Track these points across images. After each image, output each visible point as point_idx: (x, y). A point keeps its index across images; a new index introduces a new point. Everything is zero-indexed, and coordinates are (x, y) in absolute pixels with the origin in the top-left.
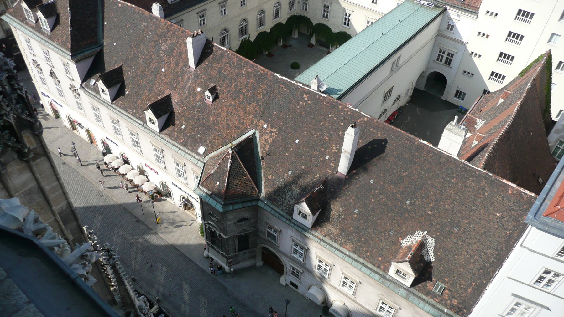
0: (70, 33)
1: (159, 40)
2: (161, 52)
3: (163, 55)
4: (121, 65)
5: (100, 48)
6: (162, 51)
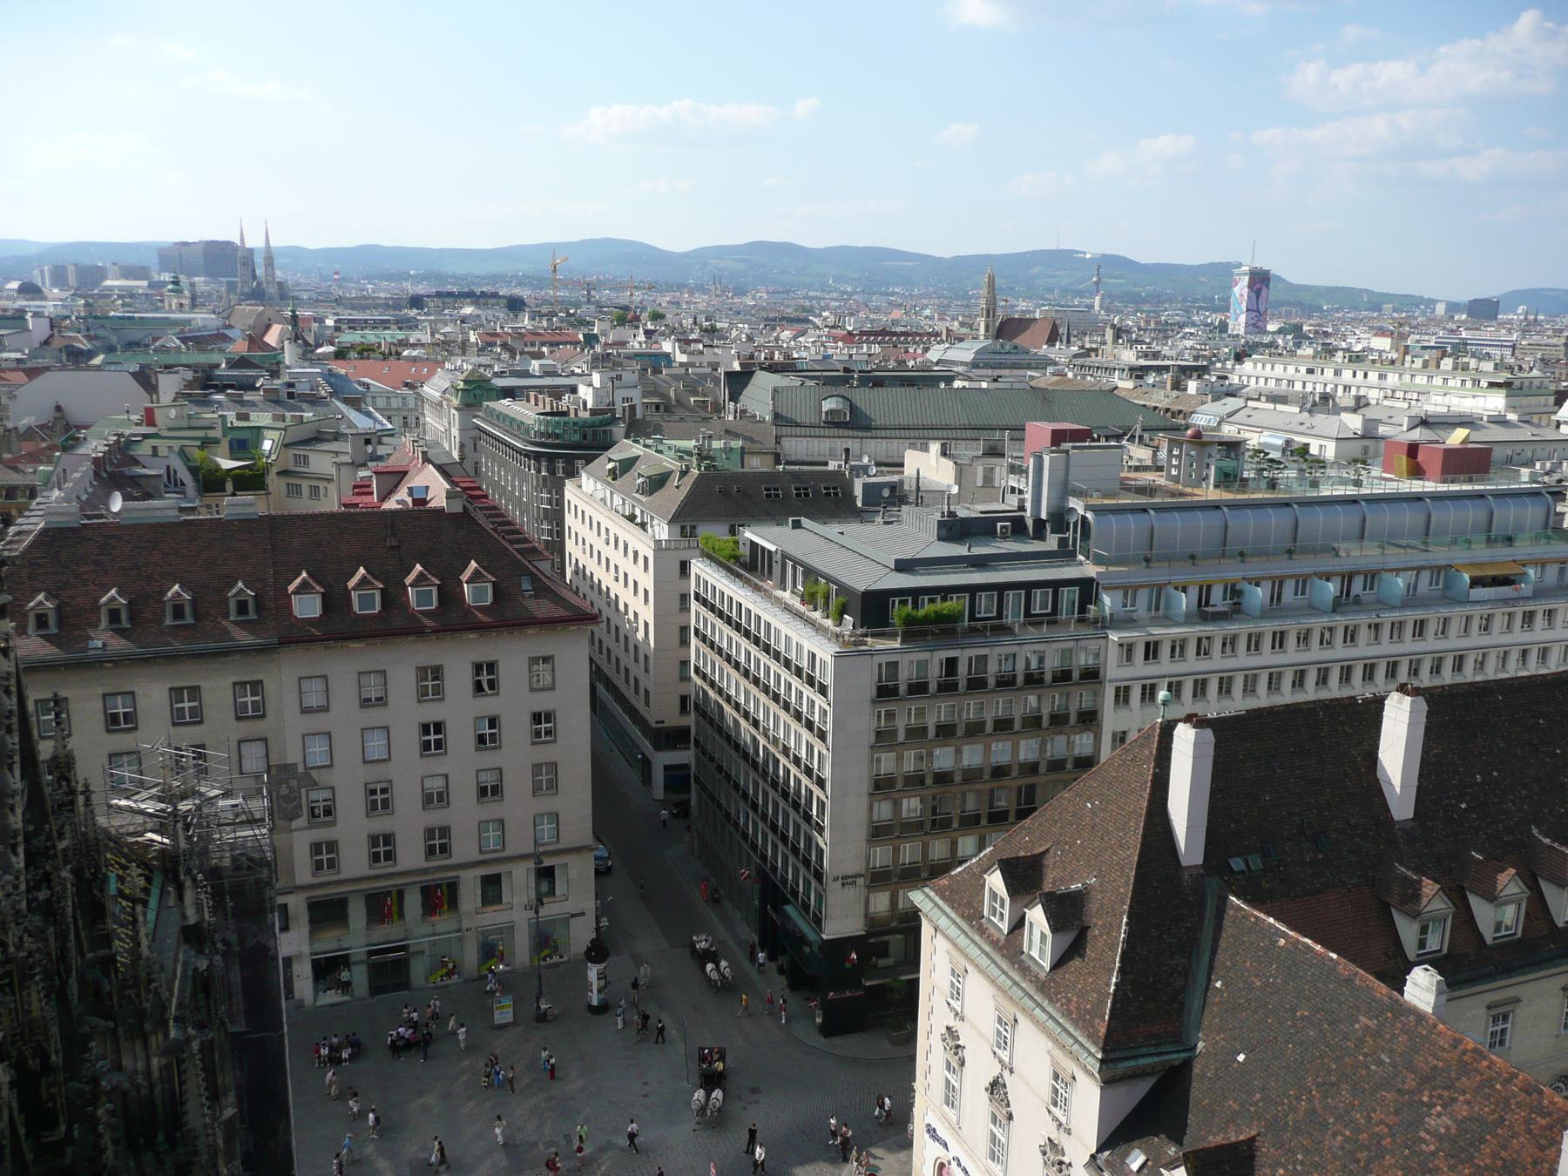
0: (1111, 991)
1: (1421, 1092)
2: (1422, 1134)
3: (1432, 1148)
4: (1253, 1133)
5: (1183, 1055)
6: (1428, 1132)
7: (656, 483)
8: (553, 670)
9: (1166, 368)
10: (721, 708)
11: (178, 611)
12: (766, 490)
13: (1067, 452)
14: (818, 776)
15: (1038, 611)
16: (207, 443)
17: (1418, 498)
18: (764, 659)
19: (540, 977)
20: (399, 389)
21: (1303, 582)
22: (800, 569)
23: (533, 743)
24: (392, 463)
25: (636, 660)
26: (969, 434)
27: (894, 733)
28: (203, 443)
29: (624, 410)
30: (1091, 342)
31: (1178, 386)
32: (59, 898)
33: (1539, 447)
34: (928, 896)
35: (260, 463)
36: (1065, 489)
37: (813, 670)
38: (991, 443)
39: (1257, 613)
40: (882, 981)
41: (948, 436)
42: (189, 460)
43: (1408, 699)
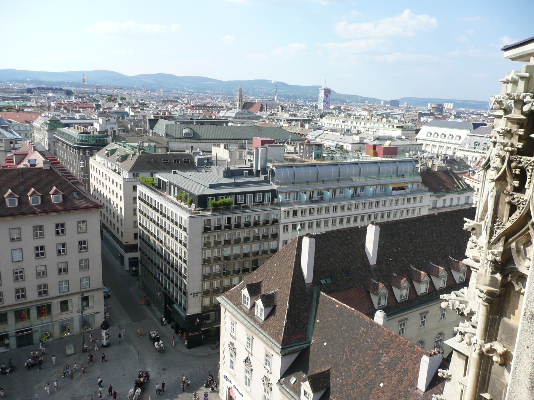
1: (379, 350)
2: (380, 363)
3: (383, 367)
4: (329, 368)
5: (307, 345)
6: (382, 362)
7: (124, 158)
8: (86, 225)
9: (298, 120)
10: (149, 237)
12: (164, 160)
13: (267, 147)
14: (184, 259)
15: (258, 201)
17: (376, 163)
18: (164, 219)
19: (84, 336)
20: (23, 123)
21: (342, 190)
22: (176, 188)
24: (21, 151)
25: (118, 221)
26: (234, 141)
27: (210, 243)
29: (111, 132)
30: (274, 111)
31: (302, 126)
33: (411, 147)
34: (223, 298)
36: (266, 160)
37: (181, 223)
38: (242, 144)
39: (328, 200)
40: (207, 328)
41: (227, 142)
43: (374, 226)
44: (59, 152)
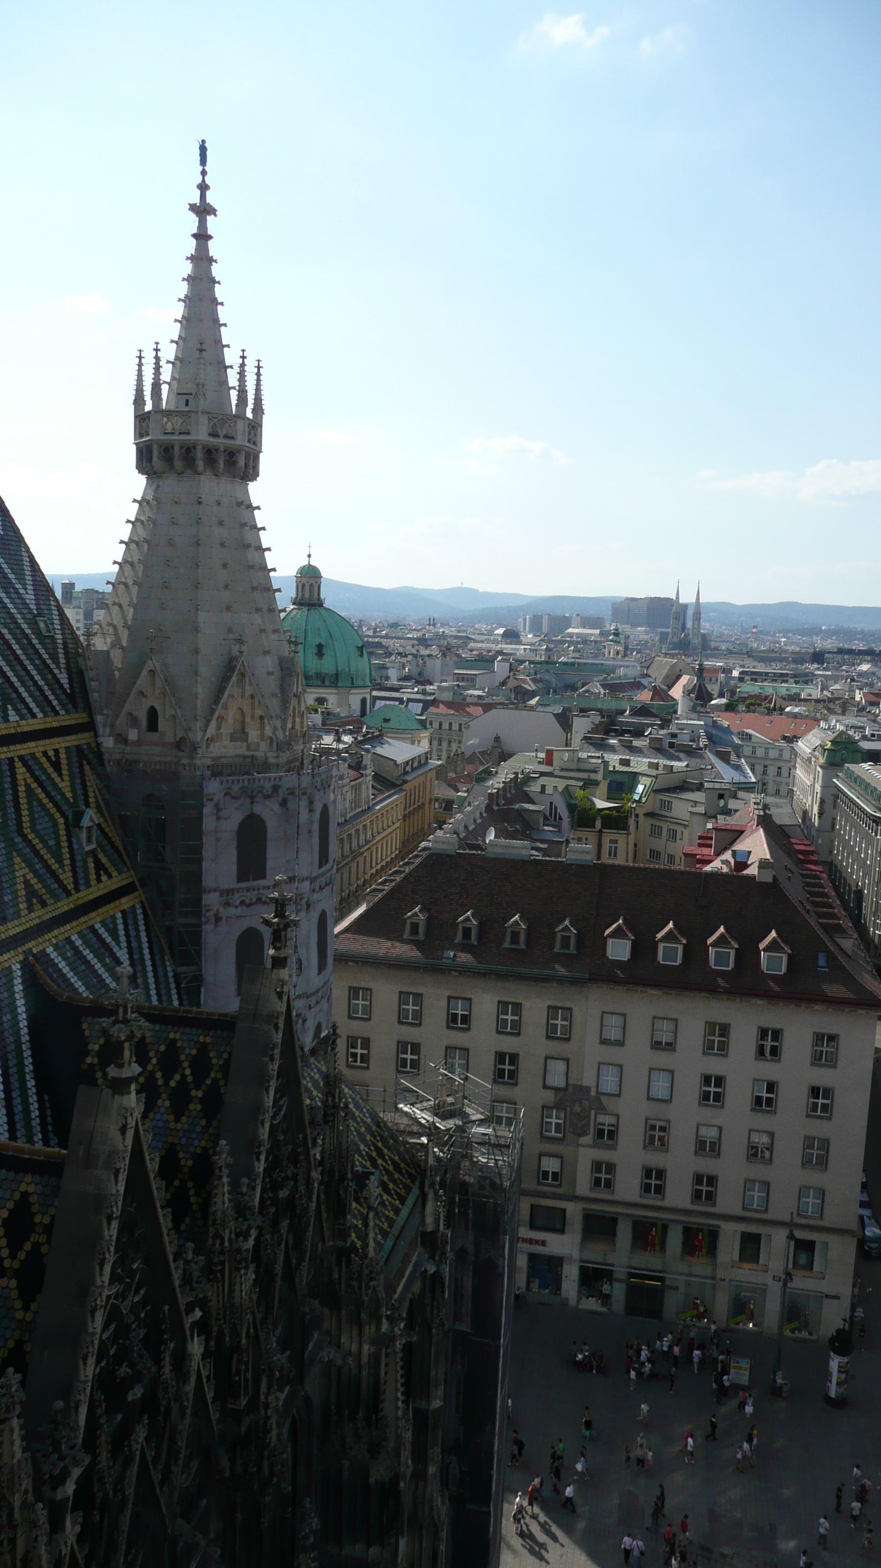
11: (515, 937)
16: (589, 784)
20: (778, 741)
23: (808, 1116)
24: (732, 821)
28: (584, 784)
32: (301, 1196)
35: (626, 807)
42: (571, 798)
44: (841, 825)
